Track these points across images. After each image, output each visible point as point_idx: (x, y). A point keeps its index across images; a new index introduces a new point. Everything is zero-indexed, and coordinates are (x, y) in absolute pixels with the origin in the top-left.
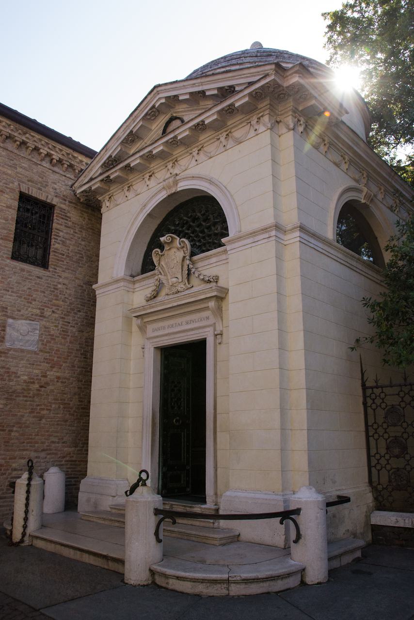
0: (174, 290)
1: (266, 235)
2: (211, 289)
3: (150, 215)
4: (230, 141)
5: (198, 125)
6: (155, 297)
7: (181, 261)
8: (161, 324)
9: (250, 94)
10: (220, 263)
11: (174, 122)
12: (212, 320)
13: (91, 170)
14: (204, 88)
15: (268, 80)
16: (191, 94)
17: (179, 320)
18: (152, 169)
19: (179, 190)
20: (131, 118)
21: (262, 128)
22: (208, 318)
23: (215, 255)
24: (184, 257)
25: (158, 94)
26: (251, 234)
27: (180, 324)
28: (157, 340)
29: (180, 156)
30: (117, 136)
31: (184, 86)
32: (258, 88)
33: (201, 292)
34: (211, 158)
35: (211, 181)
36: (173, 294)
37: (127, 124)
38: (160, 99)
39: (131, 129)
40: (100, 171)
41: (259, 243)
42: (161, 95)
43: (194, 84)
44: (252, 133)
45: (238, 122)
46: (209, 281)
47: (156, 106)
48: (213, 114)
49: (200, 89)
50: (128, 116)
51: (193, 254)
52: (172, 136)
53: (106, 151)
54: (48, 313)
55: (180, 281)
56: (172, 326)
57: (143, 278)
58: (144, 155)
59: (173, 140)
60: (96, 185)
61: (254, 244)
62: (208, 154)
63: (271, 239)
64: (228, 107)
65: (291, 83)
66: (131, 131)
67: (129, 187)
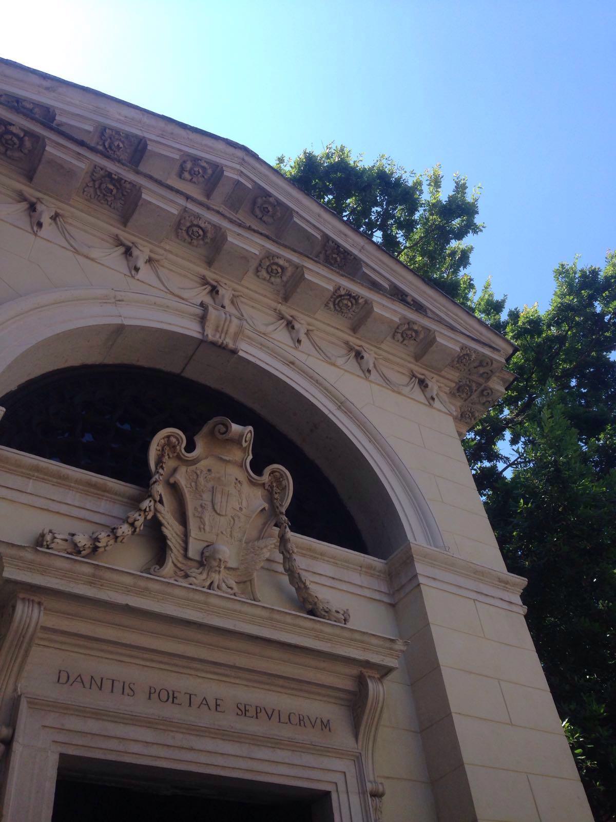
2: (388, 644)
5: (354, 298)
8: (107, 668)
10: (344, 587)
12: (342, 737)
16: (326, 238)
17: (210, 688)
18: (161, 251)
19: (241, 354)
20: (162, 124)
22: (326, 725)
23: (334, 560)
26: (476, 572)
27: (212, 704)
28: (93, 726)
29: (251, 299)
31: (319, 216)
32: (475, 351)
33: (357, 636)
34: (334, 365)
35: (342, 405)
43: (345, 235)
45: (398, 360)
49: (356, 252)
50: (161, 113)
53: (47, 89)
56: (172, 697)
57: (37, 469)
58: (198, 217)
59: (286, 265)
62: (329, 355)
64: (406, 326)
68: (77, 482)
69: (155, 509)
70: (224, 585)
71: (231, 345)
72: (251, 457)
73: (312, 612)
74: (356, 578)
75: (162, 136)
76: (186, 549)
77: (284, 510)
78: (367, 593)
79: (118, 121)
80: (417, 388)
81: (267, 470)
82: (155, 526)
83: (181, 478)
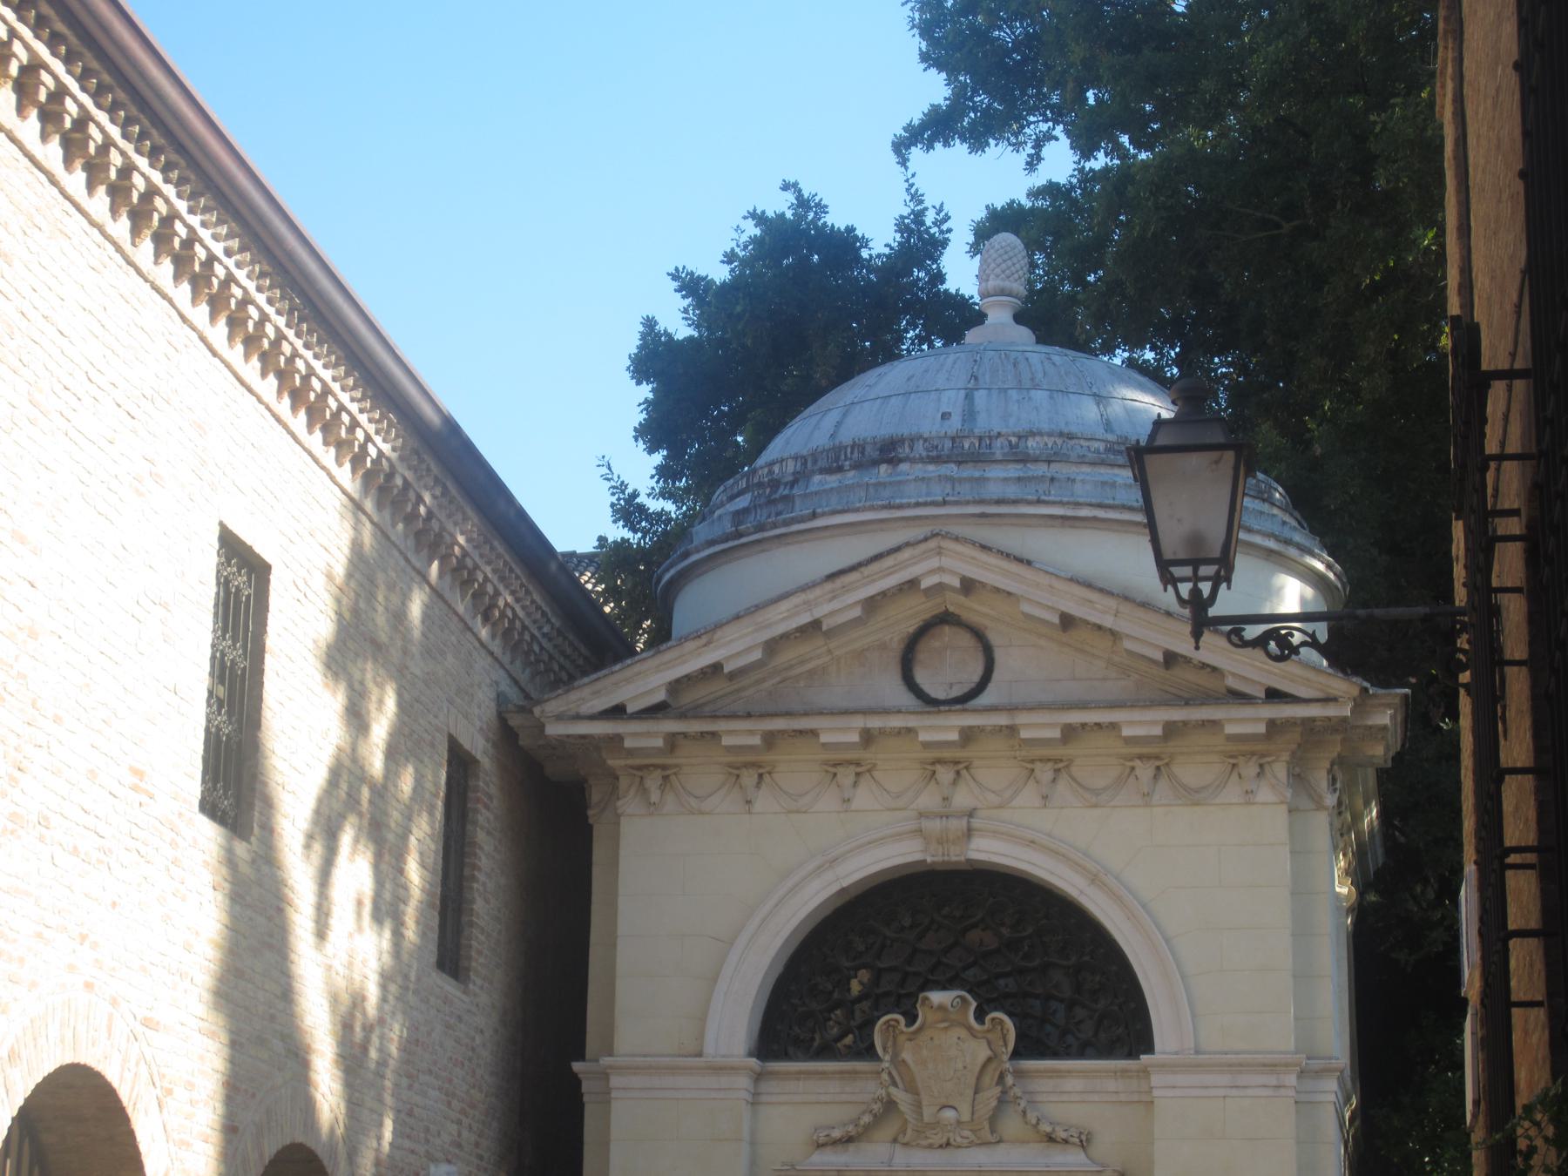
0: (938, 1139)
1: (1272, 1080)
3: (843, 890)
4: (1163, 783)
6: (849, 1140)
7: (977, 1069)
9: (1272, 724)
10: (1096, 1098)
11: (947, 629)
13: (628, 681)
14: (1122, 626)
15: (1331, 711)
20: (829, 586)
21: (1265, 794)
23: (1084, 1074)
24: (989, 1060)
25: (940, 554)
30: (760, 617)
34: (1095, 806)
36: (930, 1146)
37: (810, 595)
38: (940, 570)
39: (818, 613)
40: (660, 696)
41: (1250, 1092)
42: (946, 562)
44: (1233, 792)
46: (1066, 1141)
47: (925, 584)
48: (1154, 723)
49: (1108, 622)
51: (1016, 1054)
52: (1002, 720)
54: (465, 1134)
55: (966, 1117)
57: (800, 1073)
60: (645, 736)
61: (1234, 1092)
63: (1282, 1092)
65: (1370, 723)
66: (816, 624)
67: (761, 776)
68: (834, 1073)
69: (889, 1095)
70: (959, 1139)
71: (956, 855)
72: (974, 1004)
73: (1051, 1139)
74: (1111, 1085)
75: (834, 598)
76: (921, 1115)
77: (1005, 1057)
78: (1123, 1097)
79: (783, 620)
80: (1235, 776)
81: (988, 1018)
82: (890, 1105)
83: (906, 1055)
